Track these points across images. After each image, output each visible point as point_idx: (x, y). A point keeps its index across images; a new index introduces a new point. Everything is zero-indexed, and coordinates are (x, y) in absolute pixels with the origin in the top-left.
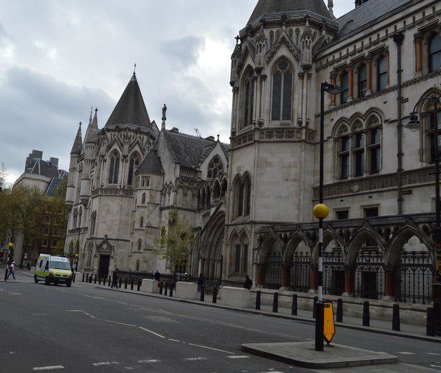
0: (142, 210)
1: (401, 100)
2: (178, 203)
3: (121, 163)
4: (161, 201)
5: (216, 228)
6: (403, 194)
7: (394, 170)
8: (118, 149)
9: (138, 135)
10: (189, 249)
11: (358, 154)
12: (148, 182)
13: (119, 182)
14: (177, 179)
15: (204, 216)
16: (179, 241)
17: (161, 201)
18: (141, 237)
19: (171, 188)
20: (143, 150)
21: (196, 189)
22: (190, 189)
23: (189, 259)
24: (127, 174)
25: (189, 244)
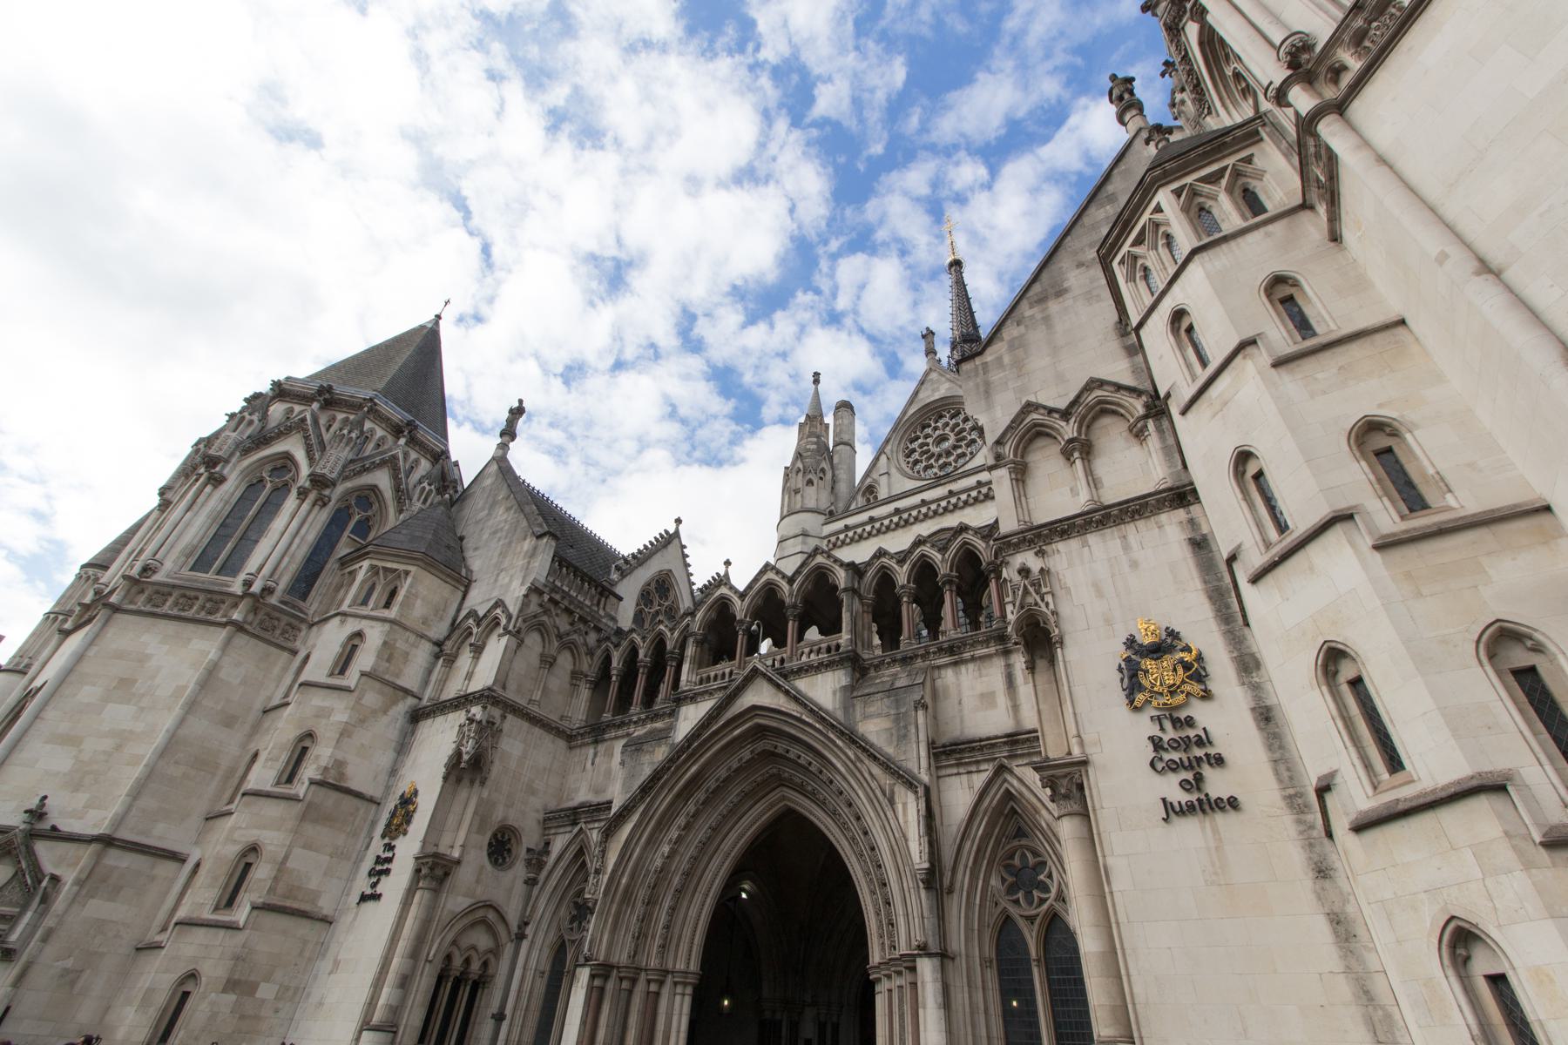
0: (318, 700)
2: (512, 685)
3: (291, 502)
4: (426, 682)
5: (700, 795)
8: (300, 455)
9: (402, 441)
10: (513, 918)
12: (393, 594)
13: (252, 565)
14: (534, 590)
15: (635, 747)
16: (474, 865)
17: (426, 682)
18: (273, 841)
20: (401, 494)
21: (591, 653)
22: (570, 647)
23: (500, 981)
24: (301, 552)
25: (520, 888)
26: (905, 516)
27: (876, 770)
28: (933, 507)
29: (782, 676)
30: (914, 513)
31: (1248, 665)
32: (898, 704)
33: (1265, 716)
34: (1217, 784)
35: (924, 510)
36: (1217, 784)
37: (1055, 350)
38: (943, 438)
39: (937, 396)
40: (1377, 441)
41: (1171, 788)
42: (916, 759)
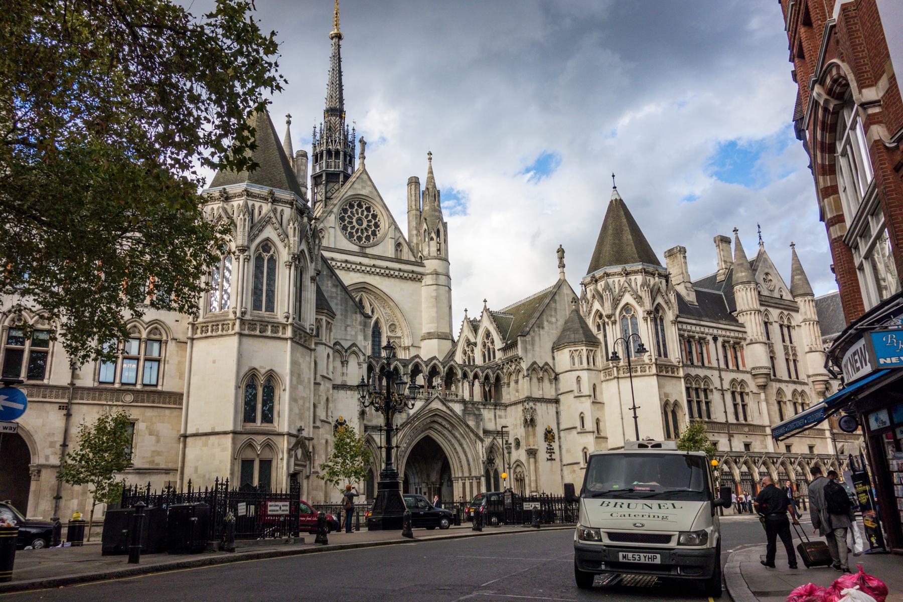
1: (721, 380)
6: (730, 436)
7: (724, 421)
11: (699, 403)
19: (354, 352)
26: (349, 266)
27: (471, 435)
28: (363, 268)
29: (444, 402)
30: (354, 266)
31: (559, 438)
32: (477, 418)
33: (560, 447)
34: (553, 457)
35: (358, 267)
36: (553, 457)
37: (540, 347)
38: (359, 221)
39: (363, 192)
40: (598, 422)
41: (548, 456)
42: (481, 434)
